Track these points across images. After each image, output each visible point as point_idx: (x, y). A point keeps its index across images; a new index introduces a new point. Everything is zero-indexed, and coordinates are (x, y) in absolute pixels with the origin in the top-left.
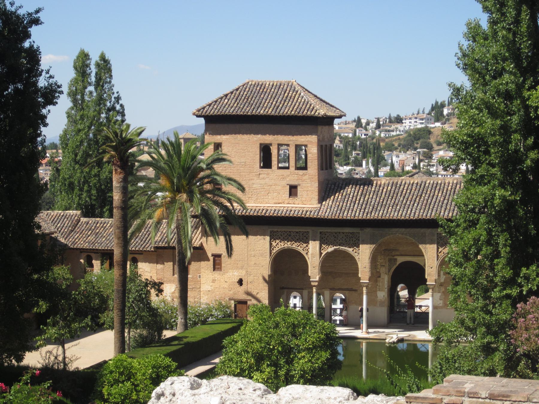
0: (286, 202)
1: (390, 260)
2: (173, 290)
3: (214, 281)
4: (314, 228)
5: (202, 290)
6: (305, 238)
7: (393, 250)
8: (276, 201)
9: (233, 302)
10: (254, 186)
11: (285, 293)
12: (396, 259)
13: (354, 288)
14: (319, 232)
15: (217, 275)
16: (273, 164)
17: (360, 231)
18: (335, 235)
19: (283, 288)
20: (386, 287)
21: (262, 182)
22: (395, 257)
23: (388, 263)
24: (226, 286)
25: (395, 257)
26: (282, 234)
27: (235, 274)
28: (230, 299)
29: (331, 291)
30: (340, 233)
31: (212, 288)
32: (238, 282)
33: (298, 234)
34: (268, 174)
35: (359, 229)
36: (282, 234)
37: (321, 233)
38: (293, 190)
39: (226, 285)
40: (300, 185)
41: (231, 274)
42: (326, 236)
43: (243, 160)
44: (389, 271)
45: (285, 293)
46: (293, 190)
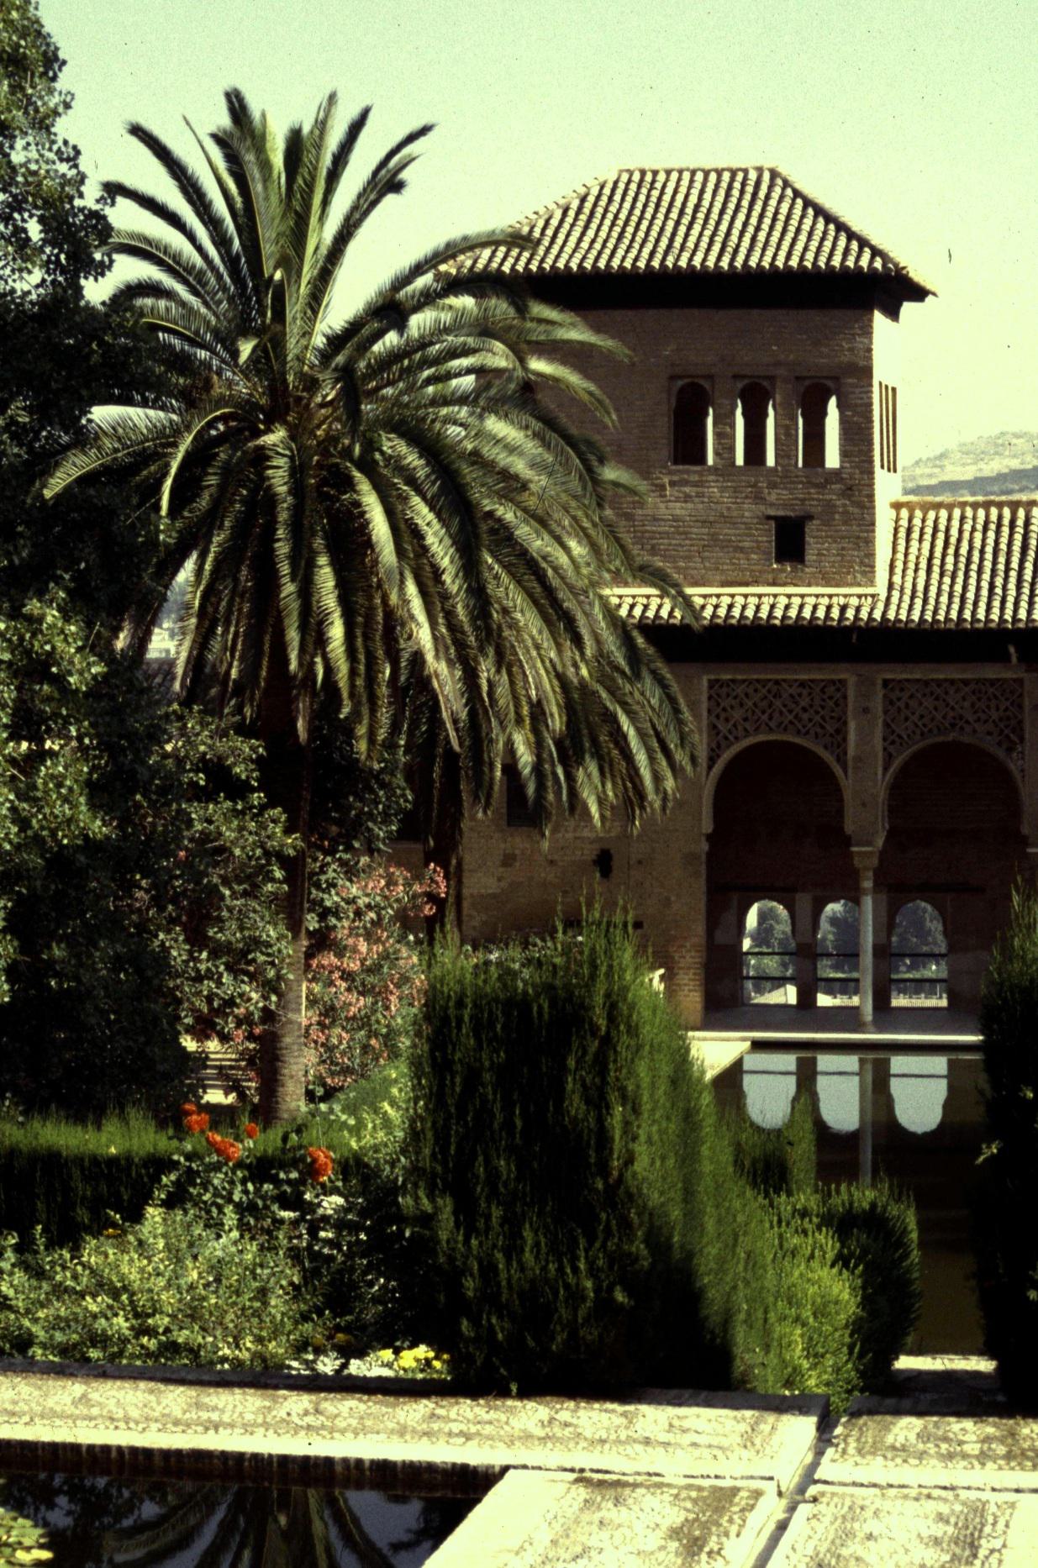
3: (508, 860)
6: (831, 703)
14: (880, 682)
15: (519, 842)
18: (939, 691)
24: (551, 877)
26: (750, 691)
30: (952, 682)
31: (503, 884)
33: (805, 692)
36: (750, 691)
37: (886, 683)
40: (811, 517)
41: (570, 835)
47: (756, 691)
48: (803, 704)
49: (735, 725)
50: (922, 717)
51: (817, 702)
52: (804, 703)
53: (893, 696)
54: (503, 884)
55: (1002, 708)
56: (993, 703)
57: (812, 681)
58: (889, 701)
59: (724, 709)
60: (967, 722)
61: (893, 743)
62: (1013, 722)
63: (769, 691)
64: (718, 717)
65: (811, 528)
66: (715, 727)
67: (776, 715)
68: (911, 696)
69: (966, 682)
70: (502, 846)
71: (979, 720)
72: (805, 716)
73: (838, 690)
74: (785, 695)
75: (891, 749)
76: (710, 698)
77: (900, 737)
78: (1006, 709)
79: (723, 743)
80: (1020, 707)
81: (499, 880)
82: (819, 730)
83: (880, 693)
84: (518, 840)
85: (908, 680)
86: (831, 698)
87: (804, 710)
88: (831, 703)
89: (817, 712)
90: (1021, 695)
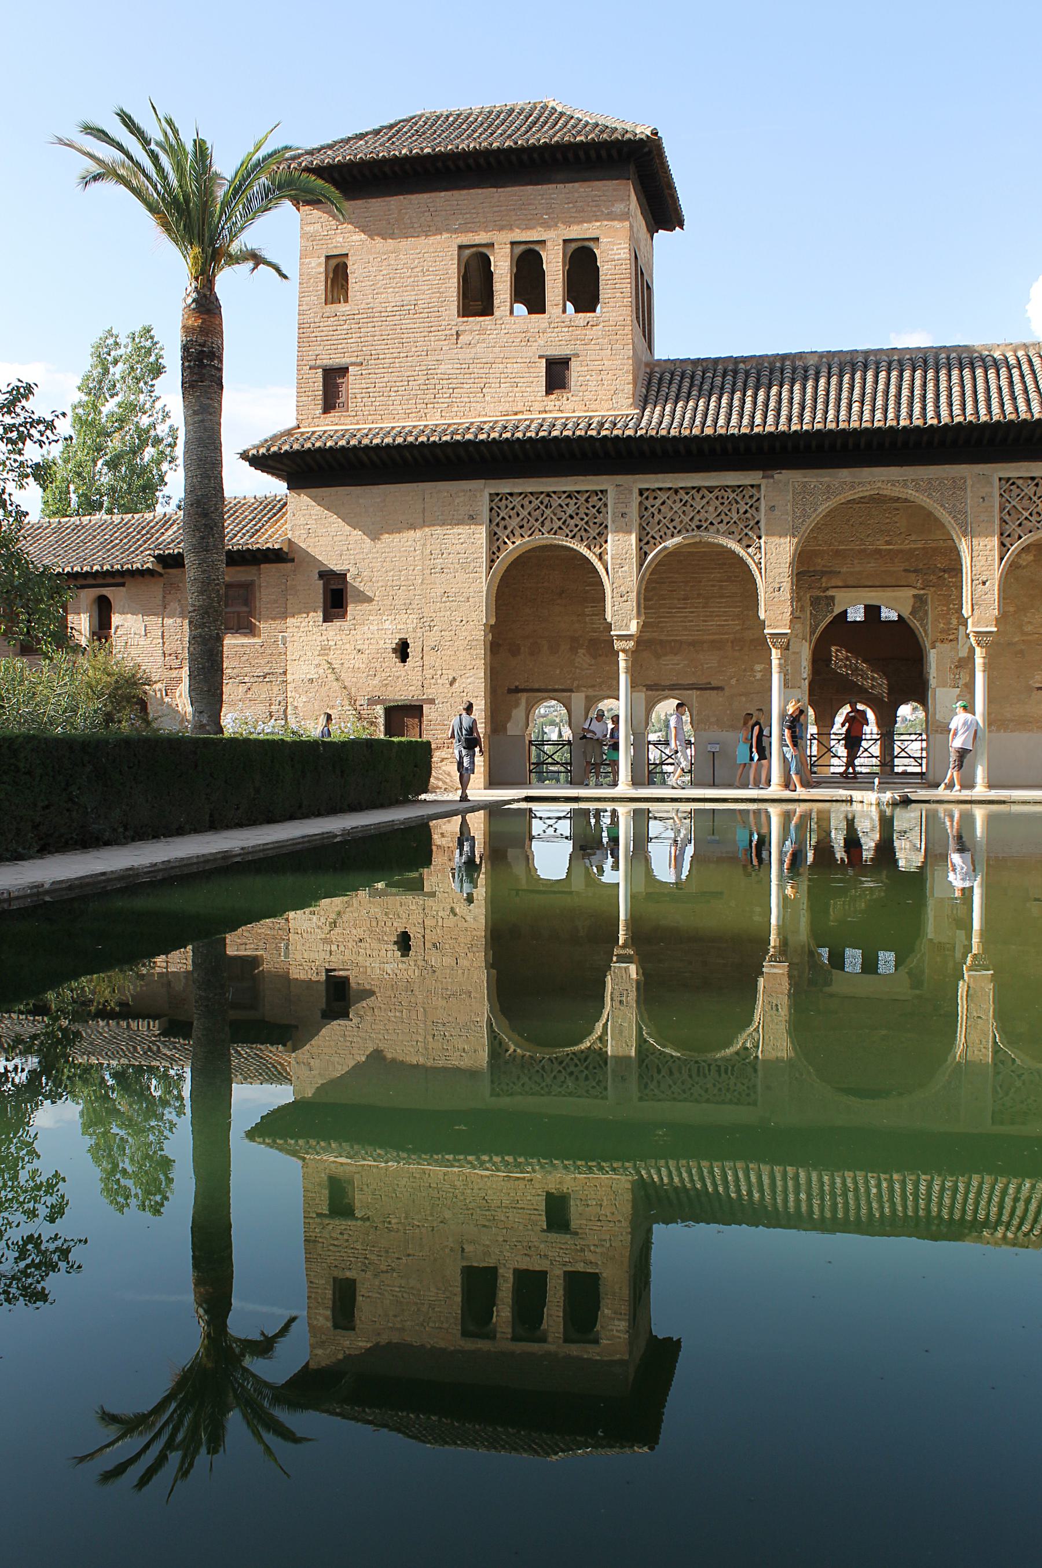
0: (537, 406)
1: (815, 602)
3: (325, 650)
4: (619, 479)
5: (289, 677)
6: (594, 511)
7: (823, 573)
8: (506, 407)
10: (443, 368)
11: (523, 702)
12: (832, 598)
13: (715, 683)
14: (636, 492)
16: (496, 302)
17: (764, 483)
19: (517, 690)
20: (805, 676)
21: (467, 354)
22: (830, 593)
23: (808, 609)
25: (830, 593)
26: (526, 502)
29: (650, 693)
32: (395, 651)
33: (573, 502)
34: (482, 331)
35: (760, 474)
38: (557, 374)
40: (577, 355)
42: (658, 502)
43: (409, 297)
44: (813, 633)
45: (523, 702)
46: (557, 374)
47: (530, 502)
48: (569, 512)
49: (512, 532)
50: (672, 520)
51: (582, 511)
52: (570, 511)
53: (647, 504)
55: (742, 511)
56: (734, 506)
57: (578, 492)
58: (643, 508)
59: (503, 519)
60: (712, 524)
61: (648, 543)
62: (752, 523)
63: (542, 503)
64: (498, 525)
65: (573, 364)
66: (495, 534)
67: (547, 523)
68: (663, 503)
69: (711, 490)
71: (722, 521)
72: (572, 522)
73: (600, 499)
74: (555, 505)
75: (646, 548)
76: (491, 509)
77: (653, 538)
78: (746, 512)
80: (757, 509)
82: (583, 534)
83: (636, 498)
85: (660, 489)
86: (594, 507)
87: (571, 517)
88: (594, 511)
89: (582, 519)
90: (758, 499)
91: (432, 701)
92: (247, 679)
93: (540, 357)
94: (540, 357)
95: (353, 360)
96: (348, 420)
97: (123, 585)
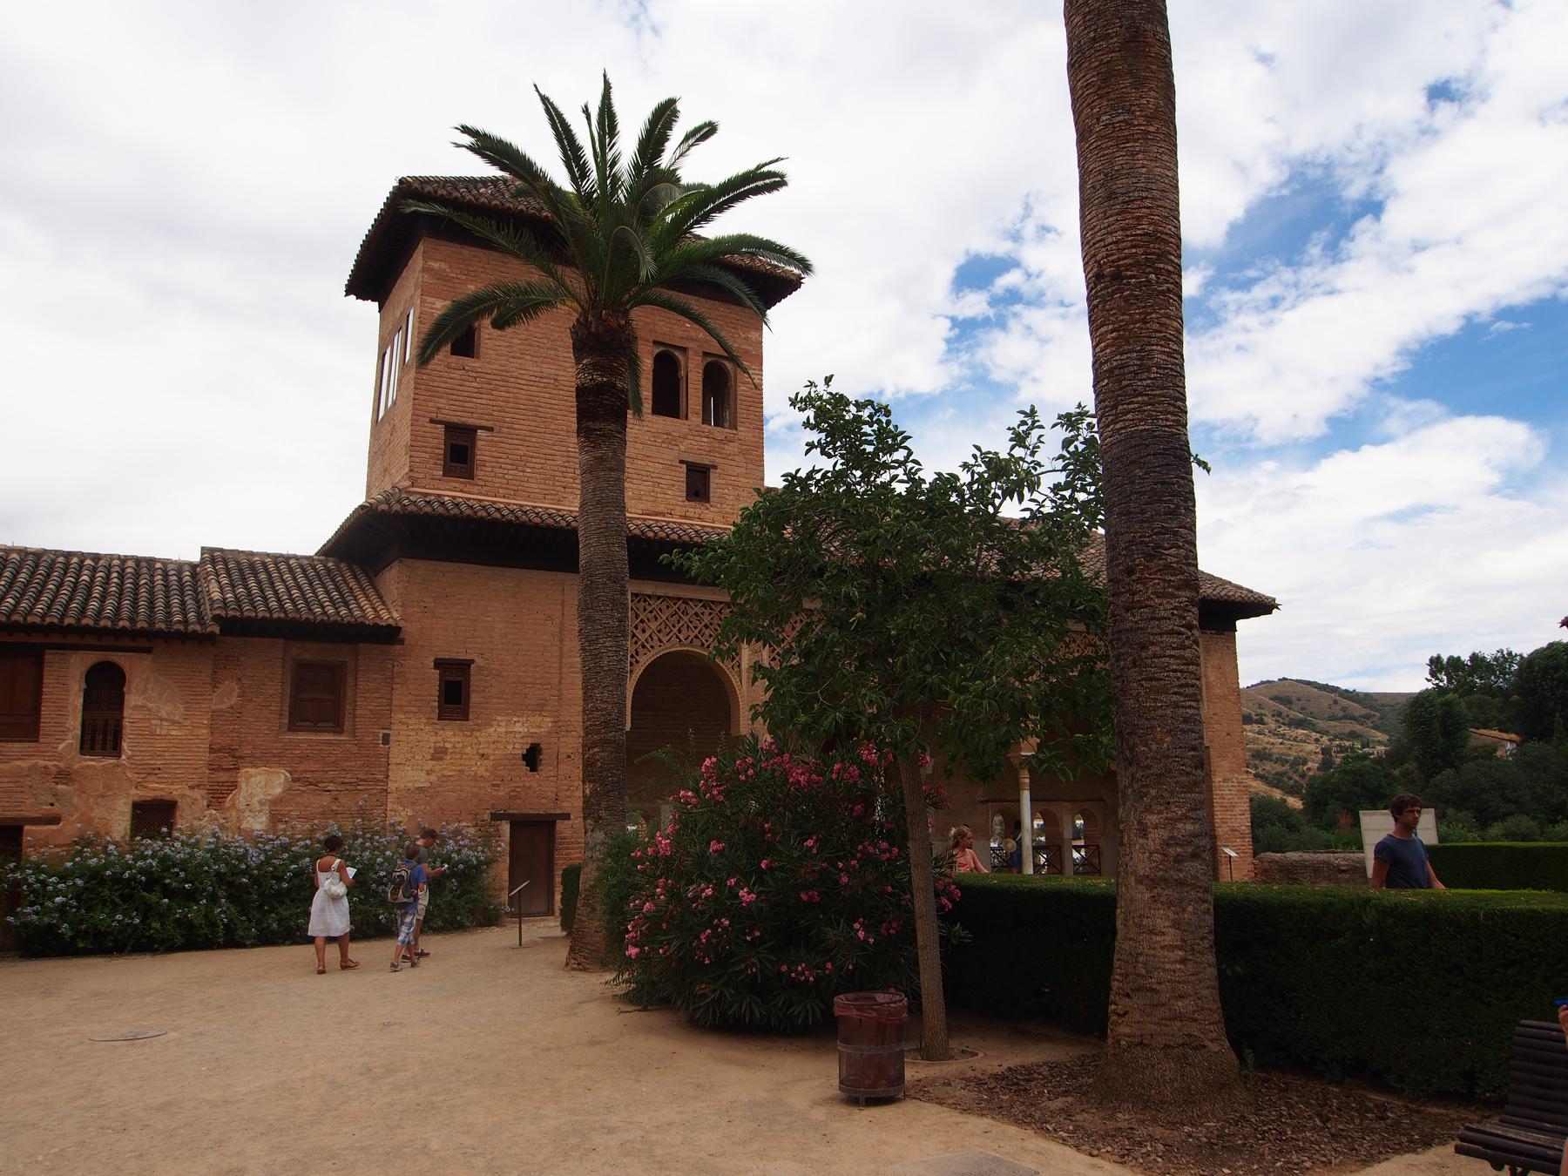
0: (678, 510)
2: (278, 790)
3: (439, 754)
5: (392, 786)
8: (650, 506)
9: (506, 827)
15: (451, 735)
24: (482, 771)
27: (518, 728)
28: (496, 817)
31: (433, 778)
36: (664, 607)
39: (482, 769)
51: (716, 621)
54: (433, 778)
67: (684, 630)
70: (433, 739)
72: (707, 632)
74: (691, 612)
79: (641, 650)
81: (428, 773)
84: (449, 733)
87: (706, 627)
91: (566, 817)
92: (331, 787)
93: (682, 462)
94: (682, 462)
95: (484, 423)
96: (475, 489)
97: (149, 651)
